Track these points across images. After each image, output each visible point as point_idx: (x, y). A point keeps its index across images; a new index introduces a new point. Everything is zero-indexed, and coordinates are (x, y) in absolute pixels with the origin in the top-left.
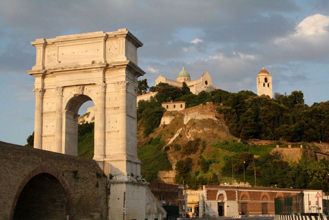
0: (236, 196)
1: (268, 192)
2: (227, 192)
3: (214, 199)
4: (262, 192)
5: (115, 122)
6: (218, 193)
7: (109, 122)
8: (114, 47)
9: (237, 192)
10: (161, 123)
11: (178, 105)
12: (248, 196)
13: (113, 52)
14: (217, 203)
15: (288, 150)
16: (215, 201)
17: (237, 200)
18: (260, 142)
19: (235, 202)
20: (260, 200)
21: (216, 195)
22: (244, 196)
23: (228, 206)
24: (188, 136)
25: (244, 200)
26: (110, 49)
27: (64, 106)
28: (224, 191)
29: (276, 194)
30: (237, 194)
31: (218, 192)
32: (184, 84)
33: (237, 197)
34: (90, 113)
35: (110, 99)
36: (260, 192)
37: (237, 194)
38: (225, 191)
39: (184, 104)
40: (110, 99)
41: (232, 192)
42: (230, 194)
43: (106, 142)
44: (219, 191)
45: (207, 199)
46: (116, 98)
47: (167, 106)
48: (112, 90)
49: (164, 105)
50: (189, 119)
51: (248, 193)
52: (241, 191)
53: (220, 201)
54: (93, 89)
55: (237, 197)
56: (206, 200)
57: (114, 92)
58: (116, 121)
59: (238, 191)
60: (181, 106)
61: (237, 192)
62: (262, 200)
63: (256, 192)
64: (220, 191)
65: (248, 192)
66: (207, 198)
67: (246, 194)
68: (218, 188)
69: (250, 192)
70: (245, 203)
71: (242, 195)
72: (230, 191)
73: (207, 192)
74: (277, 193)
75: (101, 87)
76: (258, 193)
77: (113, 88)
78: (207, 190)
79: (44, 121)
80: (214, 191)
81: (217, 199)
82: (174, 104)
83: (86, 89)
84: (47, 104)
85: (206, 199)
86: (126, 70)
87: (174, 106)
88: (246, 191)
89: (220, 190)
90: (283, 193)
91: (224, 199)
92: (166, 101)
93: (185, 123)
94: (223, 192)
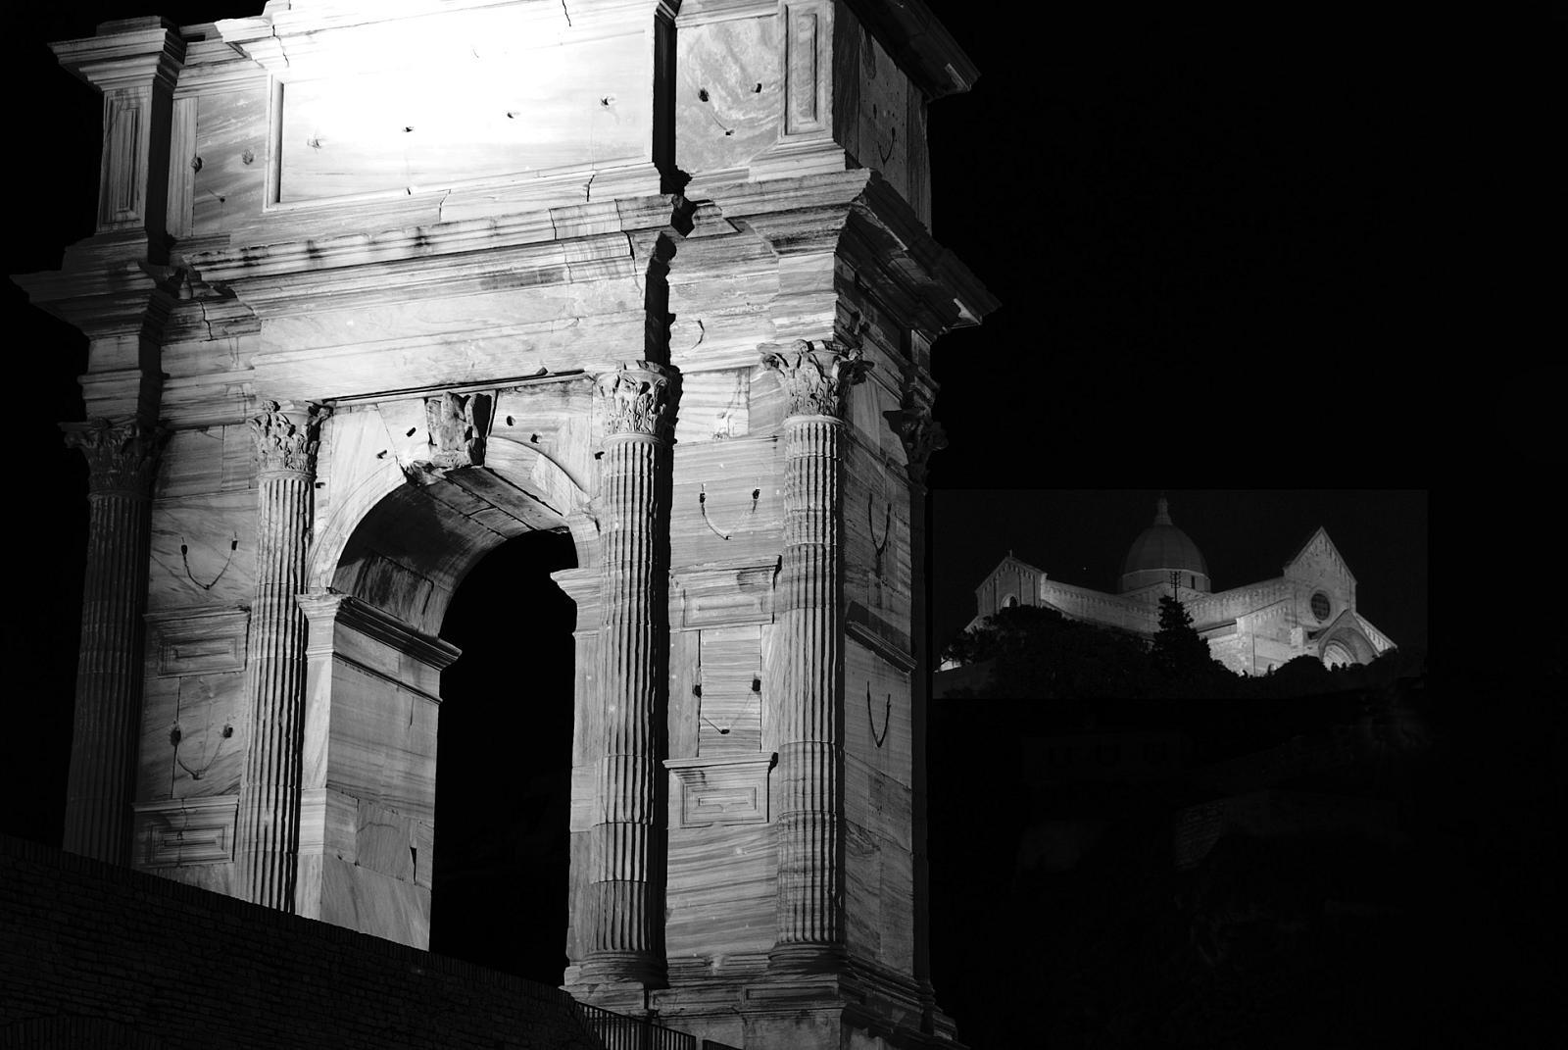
7: (697, 691)
8: (743, 69)
13: (737, 115)
26: (704, 96)
35: (702, 499)
40: (702, 499)
46: (756, 494)
48: (721, 425)
54: (564, 416)
57: (742, 437)
58: (756, 685)
75: (631, 396)
77: (730, 405)
83: (509, 421)
84: (184, 549)
86: (839, 253)
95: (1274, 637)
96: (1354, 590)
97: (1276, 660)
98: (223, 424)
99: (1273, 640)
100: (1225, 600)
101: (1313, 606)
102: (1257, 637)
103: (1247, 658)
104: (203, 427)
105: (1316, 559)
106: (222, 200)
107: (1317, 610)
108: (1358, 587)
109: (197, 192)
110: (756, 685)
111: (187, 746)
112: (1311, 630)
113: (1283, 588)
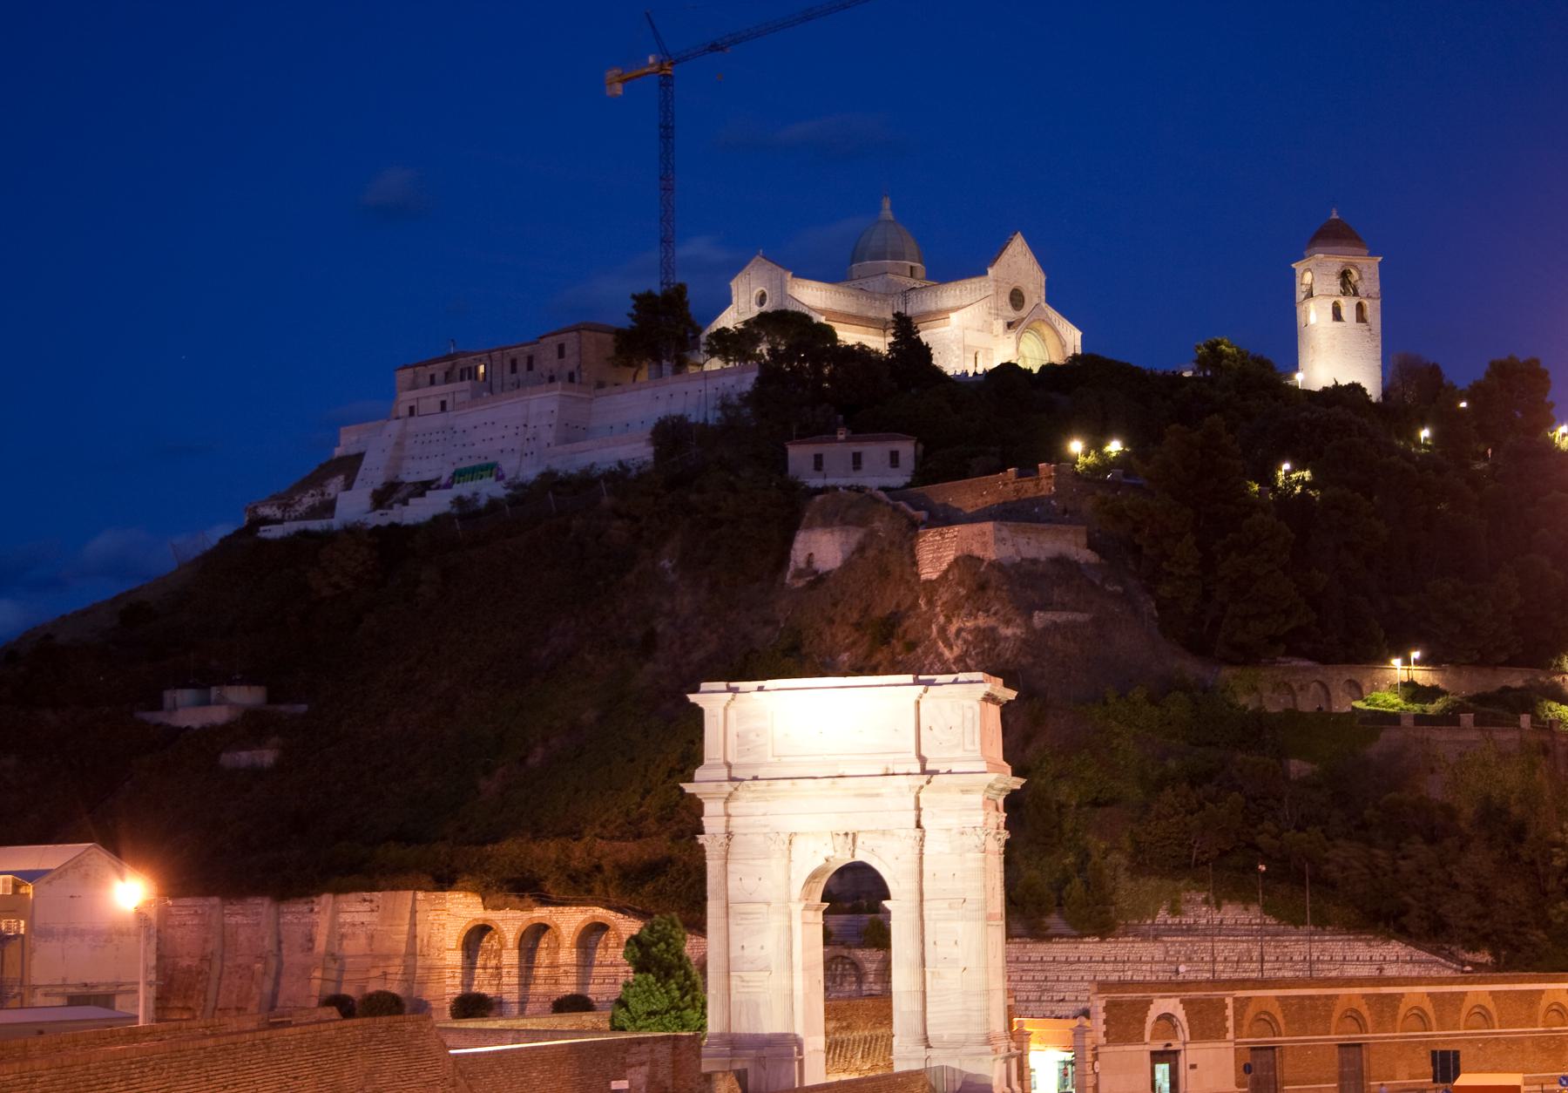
0: (1225, 1019)
1: (1364, 996)
2: (1186, 1003)
3: (1140, 1039)
4: (1337, 996)
5: (953, 943)
6: (1149, 1013)
7: (935, 943)
9: (1229, 1001)
10: (792, 563)
11: (875, 452)
12: (1279, 1017)
14: (1149, 1054)
15: (1460, 738)
16: (1141, 1047)
17: (1230, 1036)
18: (1319, 677)
19: (1223, 1045)
20: (1328, 1034)
21: (1142, 1022)
22: (1262, 1016)
23: (1193, 1067)
24: (951, 647)
25: (1262, 1036)
27: (797, 889)
28: (1178, 1000)
29: (1400, 1001)
30: (1229, 1012)
31: (1152, 1006)
32: (898, 315)
33: (1230, 1024)
34: (359, 457)
36: (1327, 997)
37: (1229, 1012)
38: (1182, 1001)
39: (907, 449)
41: (1209, 1001)
42: (1200, 1012)
43: (928, 999)
44: (1154, 1000)
45: (1108, 1041)
47: (818, 462)
49: (799, 455)
50: (950, 556)
51: (1277, 1004)
52: (1250, 998)
53: (1159, 1046)
55: (1230, 1024)
56: (1103, 1046)
58: (956, 943)
59: (1236, 1000)
60: (894, 459)
61: (1229, 1001)
62: (1336, 1034)
63: (1310, 997)
64: (1161, 1001)
65: (1277, 998)
66: (1106, 1034)
67: (1269, 1009)
68: (1159, 991)
69: (1287, 997)
70: (1262, 1048)
71: (1251, 1012)
72: (1203, 1001)
73: (1106, 1009)
74: (1402, 995)
76: (1319, 1003)
78: (1107, 1002)
79: (733, 928)
80: (1133, 1003)
81: (1147, 1038)
82: (856, 448)
84: (741, 879)
85: (1103, 1040)
87: (857, 460)
88: (1271, 997)
89: (1161, 997)
90: (1429, 994)
91: (1176, 1037)
92: (809, 433)
93: (929, 572)
94: (1170, 1005)
95: (980, 328)
96: (1044, 284)
97: (982, 348)
98: (753, 834)
99: (978, 330)
100: (939, 292)
101: (1012, 299)
102: (967, 329)
103: (958, 348)
104: (746, 835)
105: (1014, 259)
106: (748, 749)
107: (1014, 303)
108: (1047, 282)
109: (739, 745)
110: (956, 943)
111: (747, 952)
112: (1010, 320)
113: (987, 285)
